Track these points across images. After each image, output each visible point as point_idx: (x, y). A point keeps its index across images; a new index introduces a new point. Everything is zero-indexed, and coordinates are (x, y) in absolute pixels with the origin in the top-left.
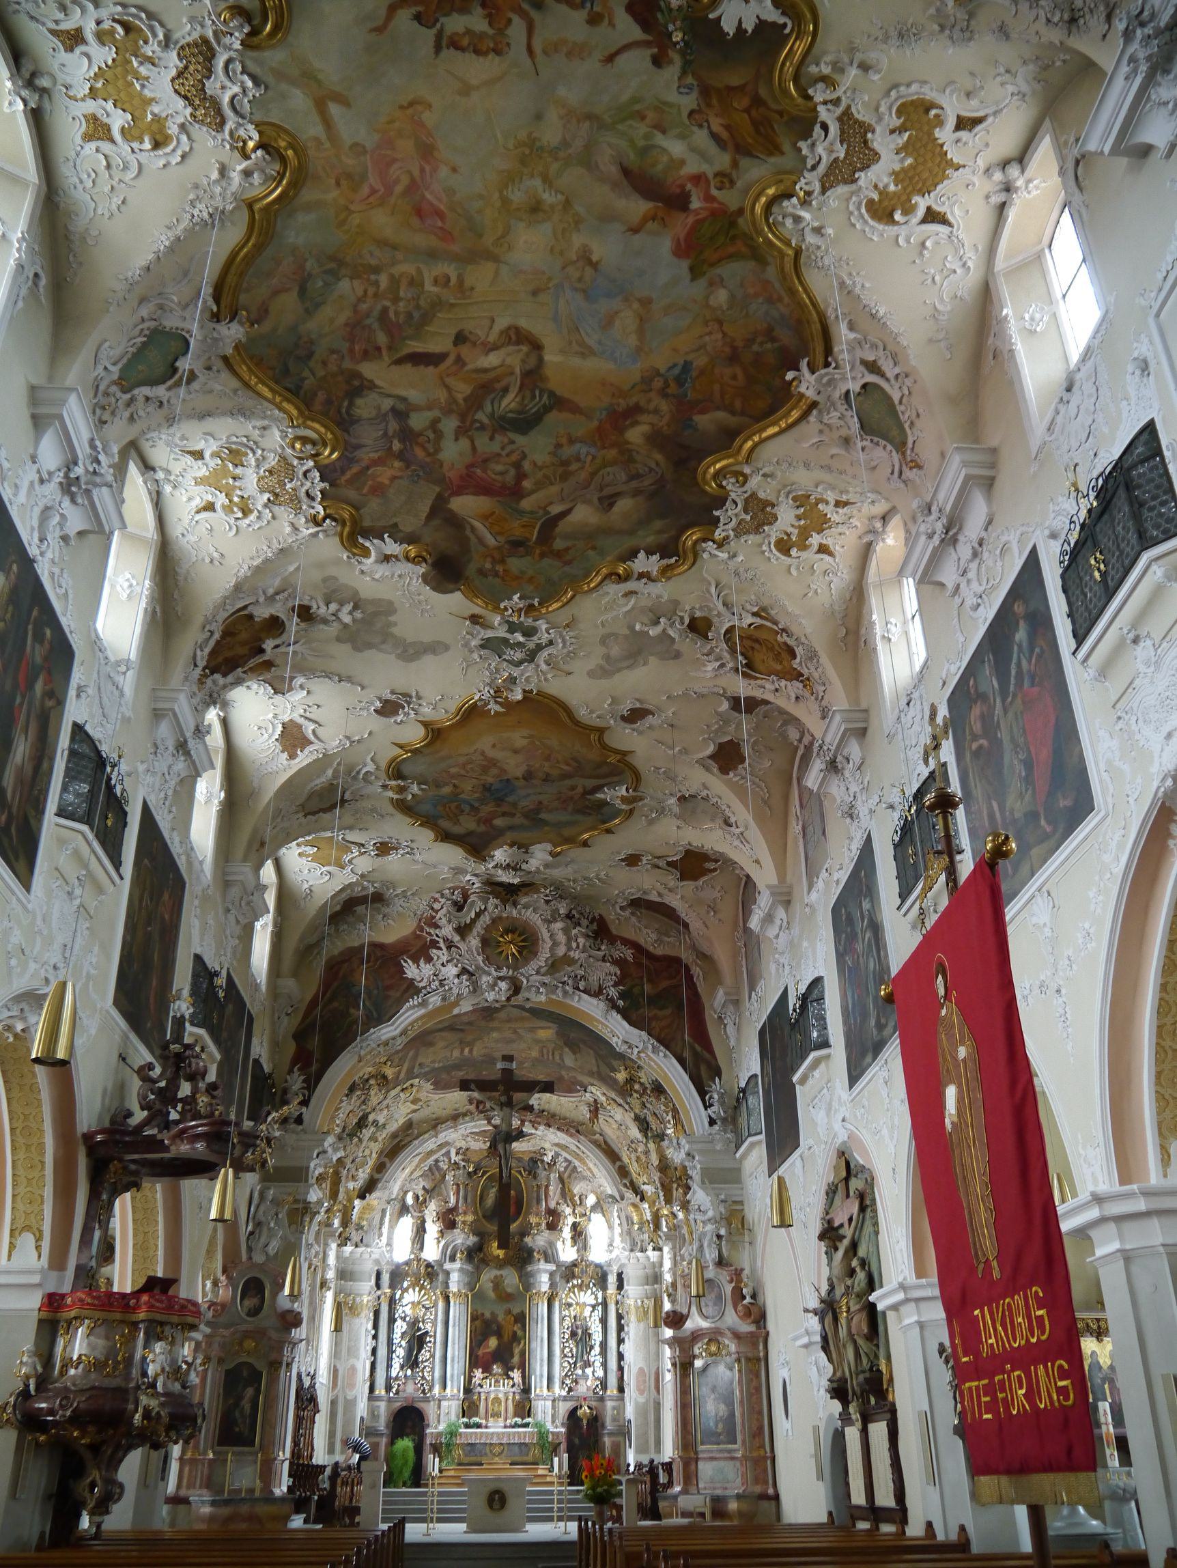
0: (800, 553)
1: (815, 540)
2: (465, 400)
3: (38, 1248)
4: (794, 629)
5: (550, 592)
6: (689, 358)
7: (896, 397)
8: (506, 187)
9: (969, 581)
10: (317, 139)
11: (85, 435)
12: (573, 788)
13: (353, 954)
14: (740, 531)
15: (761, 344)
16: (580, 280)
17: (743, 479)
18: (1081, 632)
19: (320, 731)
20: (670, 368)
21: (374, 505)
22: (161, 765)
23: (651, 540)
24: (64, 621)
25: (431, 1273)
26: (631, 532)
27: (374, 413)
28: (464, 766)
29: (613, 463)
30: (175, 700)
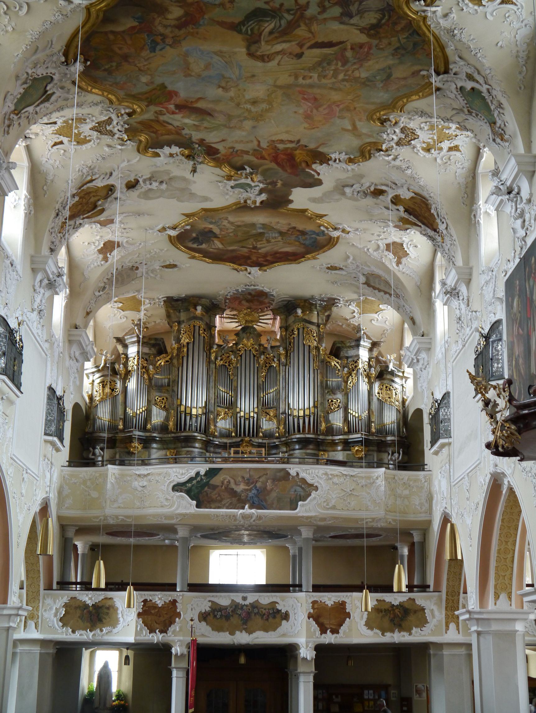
6: (153, 54)
8: (269, 108)
10: (360, 120)
15: (112, 66)
16: (227, 82)
20: (163, 48)
27: (366, 15)
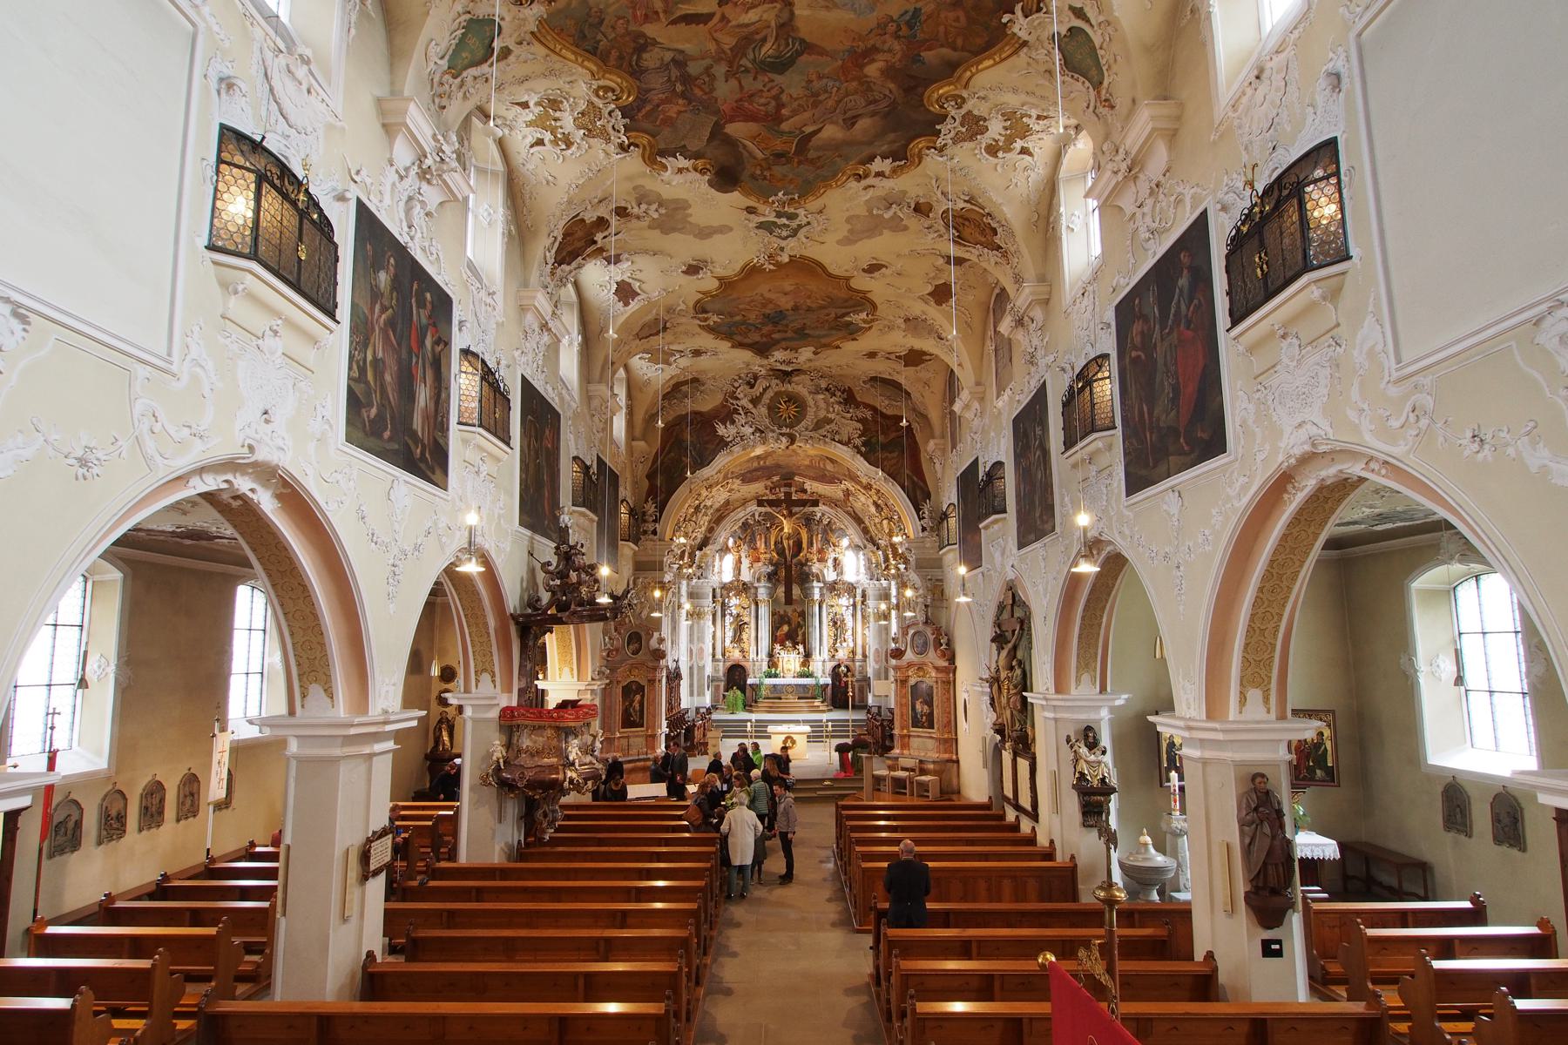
0: (1005, 155)
1: (1018, 144)
2: (731, 49)
3: (493, 681)
4: (995, 214)
5: (807, 189)
7: (1097, 41)
9: (1144, 214)
11: (429, 133)
12: (828, 315)
13: (681, 419)
14: (955, 141)
17: (960, 102)
18: (1237, 315)
19: (643, 286)
21: (666, 132)
22: (530, 345)
23: (885, 148)
24: (439, 280)
25: (744, 588)
26: (870, 143)
28: (749, 303)
29: (856, 92)
30: (534, 298)
